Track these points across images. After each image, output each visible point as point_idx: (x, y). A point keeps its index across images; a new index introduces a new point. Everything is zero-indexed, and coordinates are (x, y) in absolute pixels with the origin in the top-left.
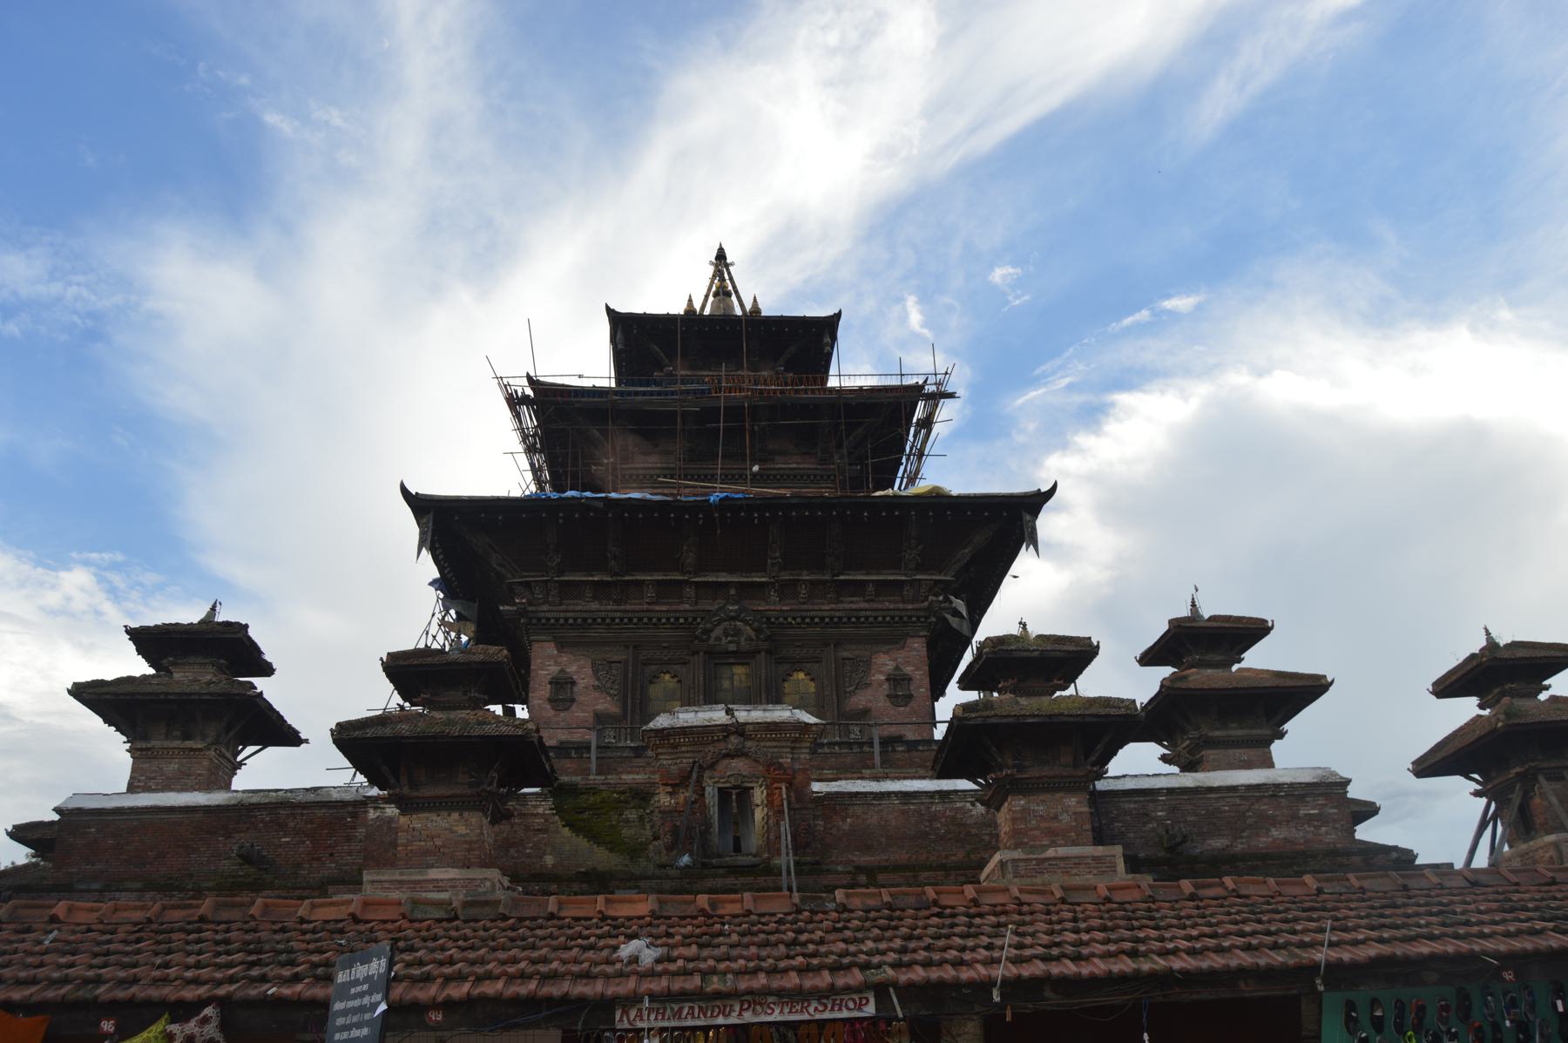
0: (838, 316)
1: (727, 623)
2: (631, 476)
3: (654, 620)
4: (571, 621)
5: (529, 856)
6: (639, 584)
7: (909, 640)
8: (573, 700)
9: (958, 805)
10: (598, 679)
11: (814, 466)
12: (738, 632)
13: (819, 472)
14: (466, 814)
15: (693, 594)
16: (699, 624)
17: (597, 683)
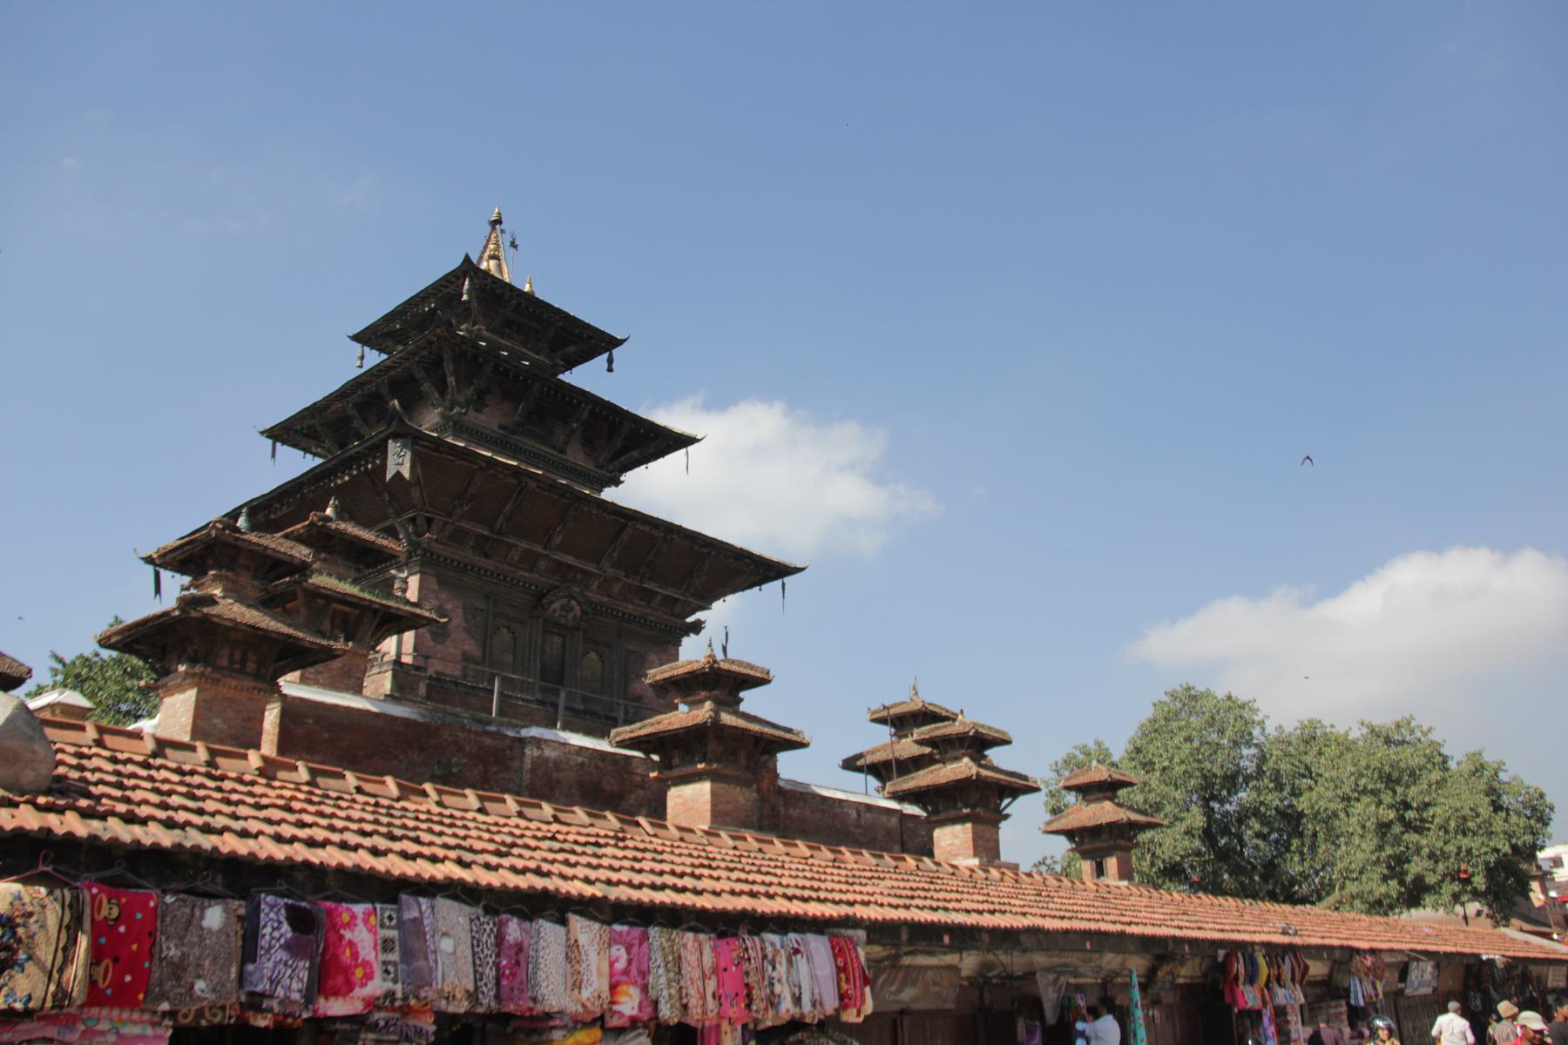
0: (625, 340)
1: (565, 600)
2: (467, 428)
3: (515, 582)
4: (455, 564)
5: (632, 805)
6: (511, 546)
7: (670, 647)
8: (448, 636)
9: (845, 810)
10: (466, 622)
11: (592, 468)
12: (572, 609)
13: (597, 476)
14: (744, 790)
15: (543, 568)
16: (543, 596)
17: (465, 625)
